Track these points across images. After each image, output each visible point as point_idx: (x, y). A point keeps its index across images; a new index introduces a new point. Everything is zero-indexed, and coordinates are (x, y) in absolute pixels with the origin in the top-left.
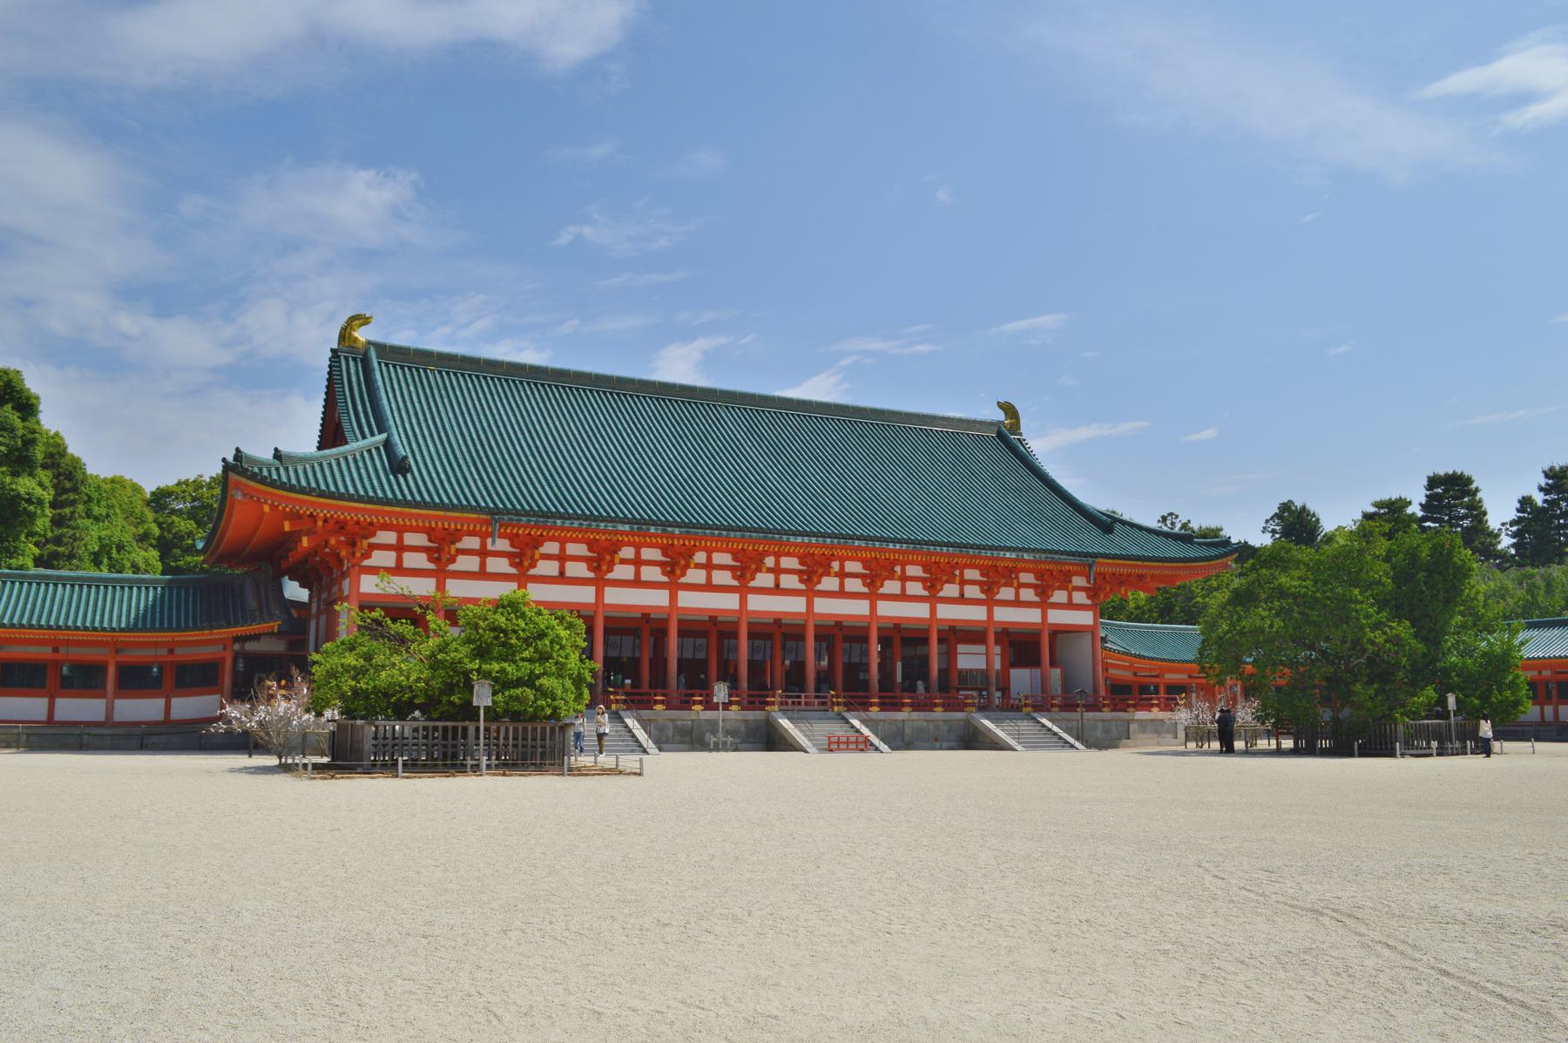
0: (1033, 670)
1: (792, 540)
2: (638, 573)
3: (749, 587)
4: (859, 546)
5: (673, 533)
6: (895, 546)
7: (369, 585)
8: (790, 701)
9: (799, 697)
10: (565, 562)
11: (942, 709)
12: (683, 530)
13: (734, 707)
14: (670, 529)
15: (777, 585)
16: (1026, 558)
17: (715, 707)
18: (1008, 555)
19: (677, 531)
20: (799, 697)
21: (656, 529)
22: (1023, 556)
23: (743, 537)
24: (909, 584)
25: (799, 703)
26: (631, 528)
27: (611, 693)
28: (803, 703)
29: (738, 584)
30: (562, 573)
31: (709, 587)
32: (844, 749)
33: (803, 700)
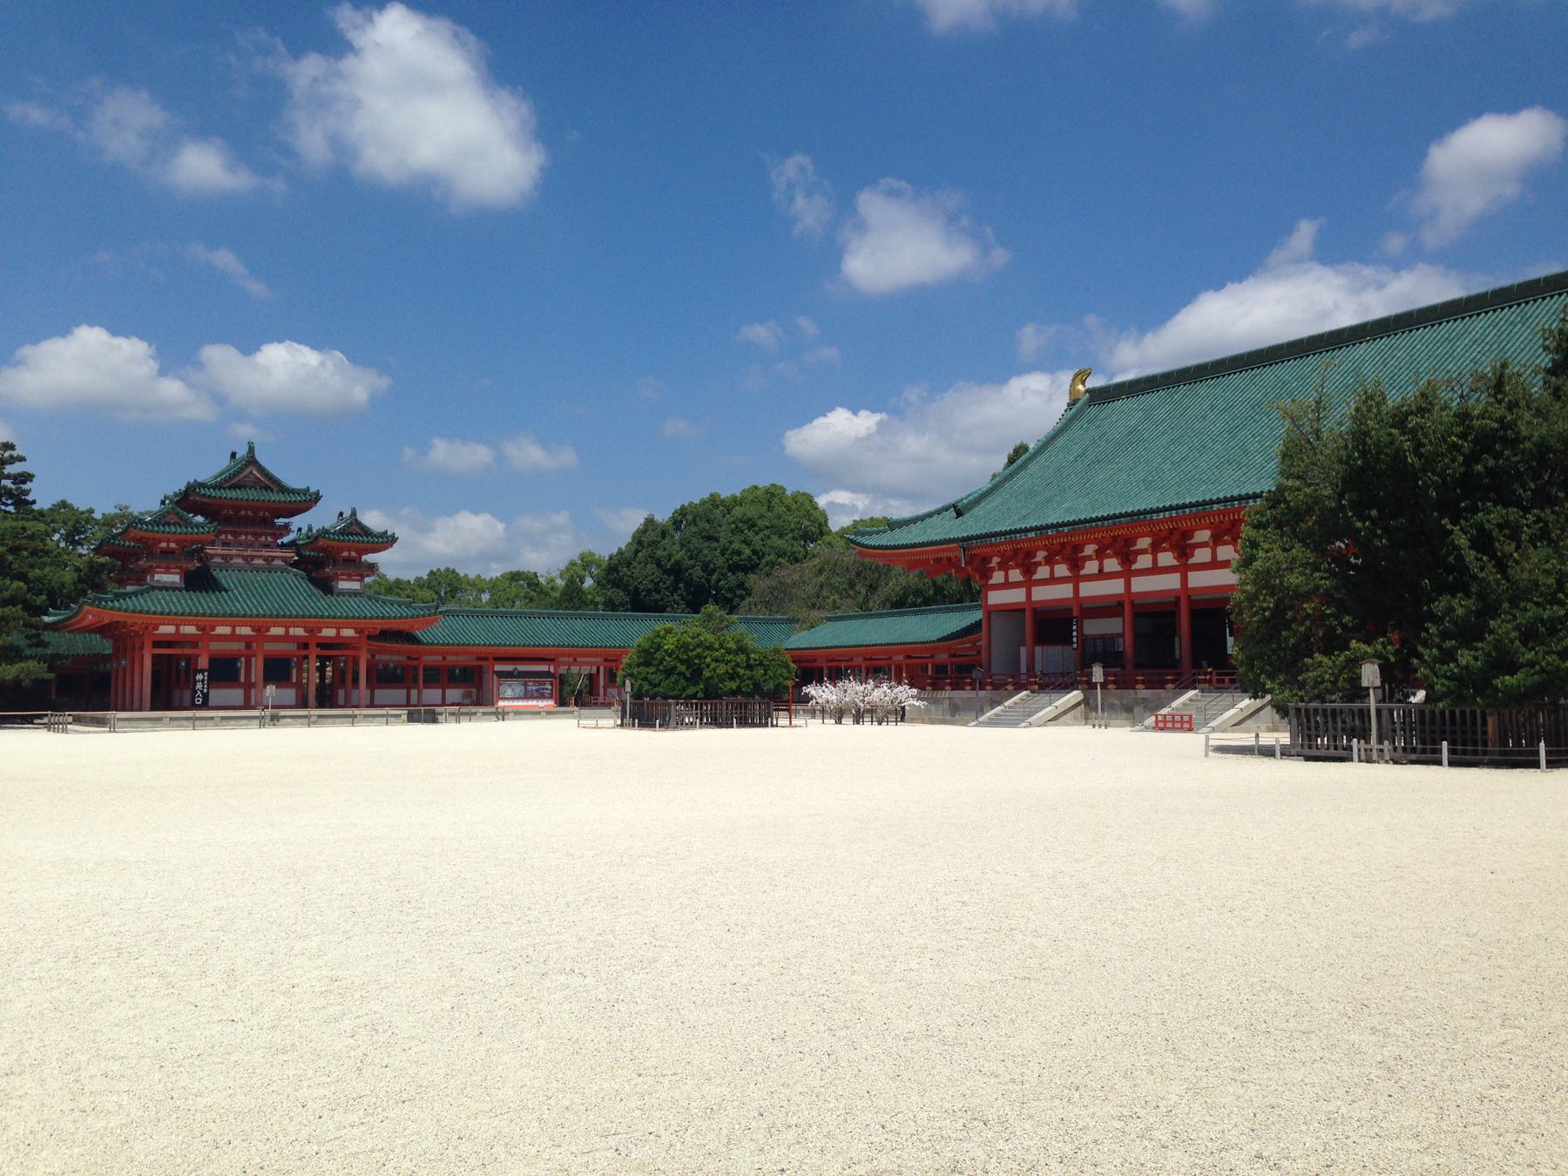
0: (1045, 648)
1: (1155, 518)
4: (1219, 510)
5: (1063, 531)
6: (1255, 502)
7: (995, 598)
8: (1227, 679)
10: (1194, 550)
11: (1143, 687)
12: (1070, 527)
13: (1170, 686)
14: (1060, 529)
19: (1066, 529)
21: (1052, 532)
23: (1114, 524)
26: (1036, 534)
30: (1101, 570)
32: (1178, 729)
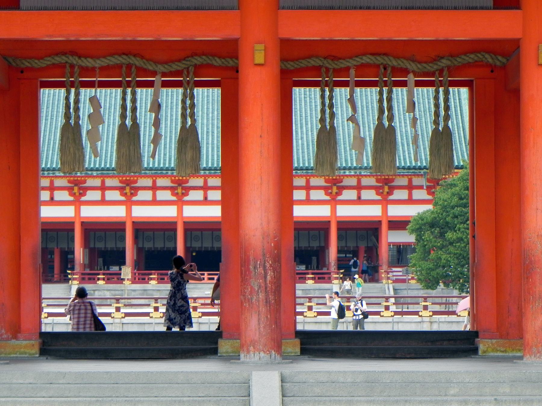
2: (103, 196)
3: (184, 201)
9: (204, 274)
14: (90, 173)
15: (206, 198)
16: (363, 174)
17: (121, 281)
18: (347, 173)
19: (95, 173)
20: (204, 274)
22: (360, 173)
24: (312, 192)
25: (204, 279)
27: (69, 274)
28: (206, 279)
29: (177, 199)
31: (154, 202)
33: (206, 276)
